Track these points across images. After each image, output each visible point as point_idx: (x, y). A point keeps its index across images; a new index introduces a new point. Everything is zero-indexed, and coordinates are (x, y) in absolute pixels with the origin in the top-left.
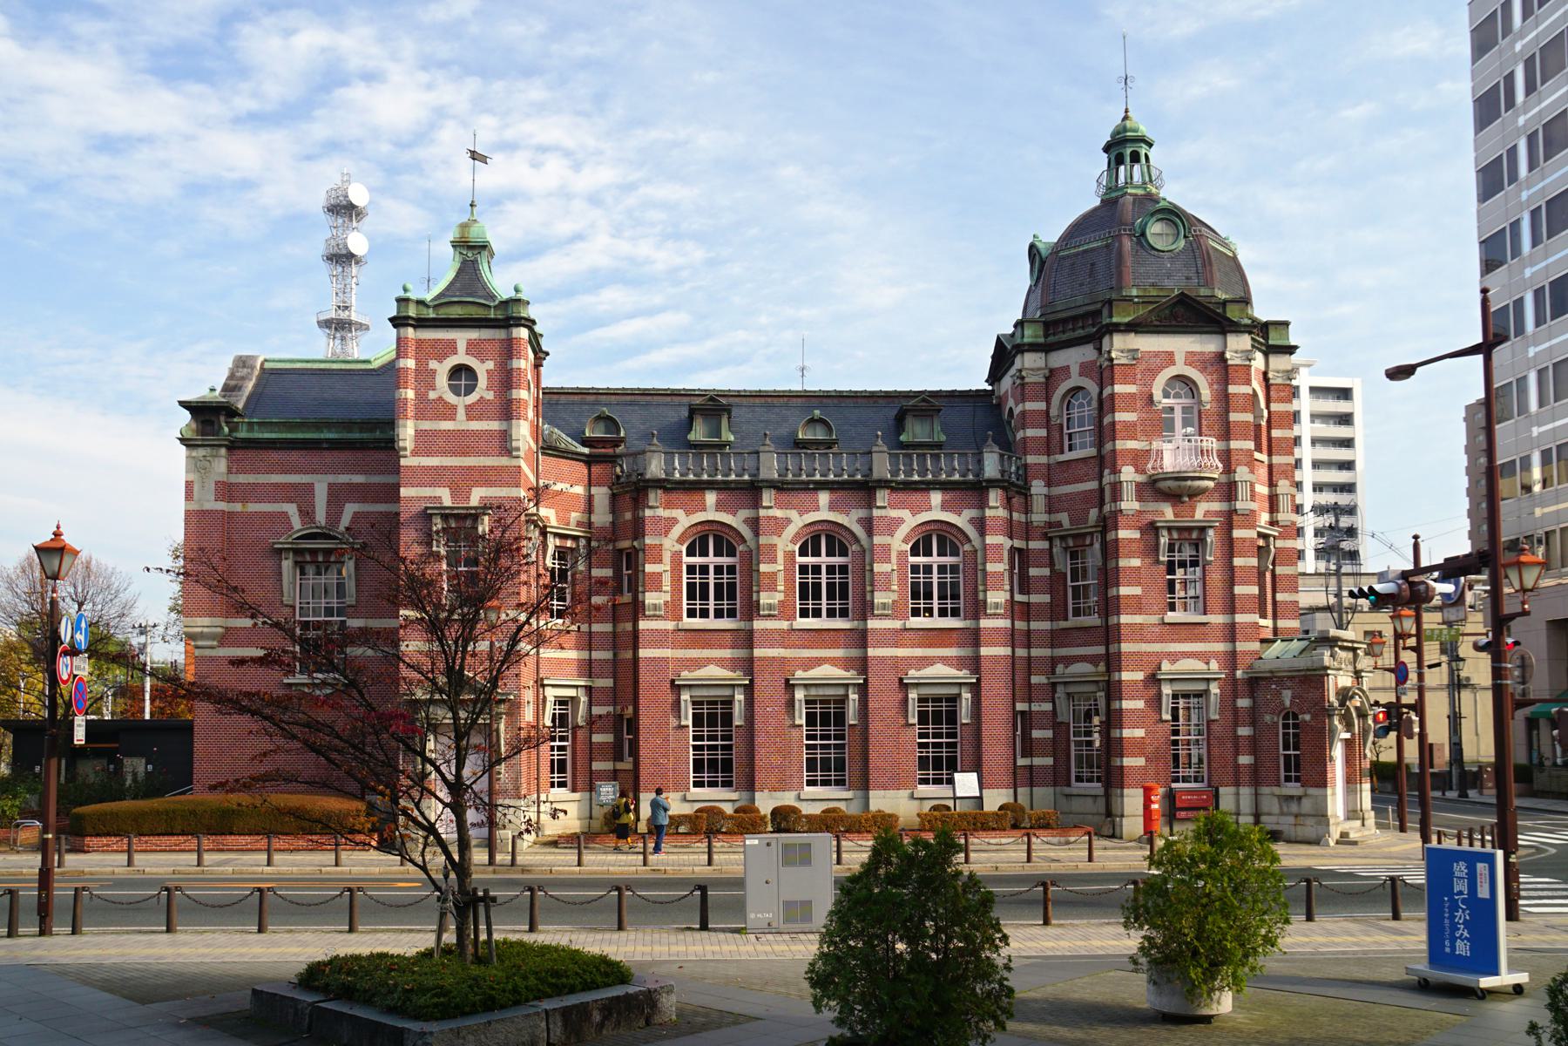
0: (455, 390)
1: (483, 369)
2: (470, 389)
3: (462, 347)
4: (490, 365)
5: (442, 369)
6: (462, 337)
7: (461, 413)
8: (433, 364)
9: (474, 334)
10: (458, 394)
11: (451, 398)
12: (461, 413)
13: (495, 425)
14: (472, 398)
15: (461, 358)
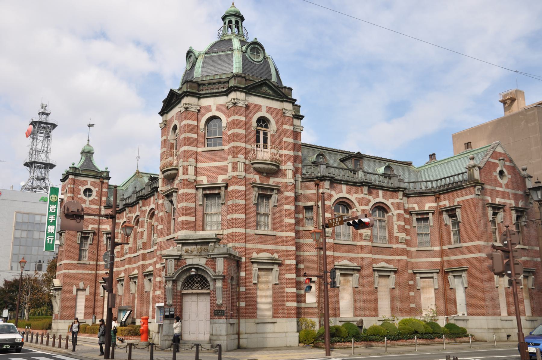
0: (85, 195)
1: (95, 191)
2: (90, 196)
3: (89, 183)
4: (97, 189)
5: (82, 189)
6: (89, 180)
7: (88, 203)
8: (80, 187)
9: (93, 180)
10: (86, 196)
11: (84, 198)
12: (88, 203)
13: (97, 207)
14: (91, 198)
15: (89, 186)
